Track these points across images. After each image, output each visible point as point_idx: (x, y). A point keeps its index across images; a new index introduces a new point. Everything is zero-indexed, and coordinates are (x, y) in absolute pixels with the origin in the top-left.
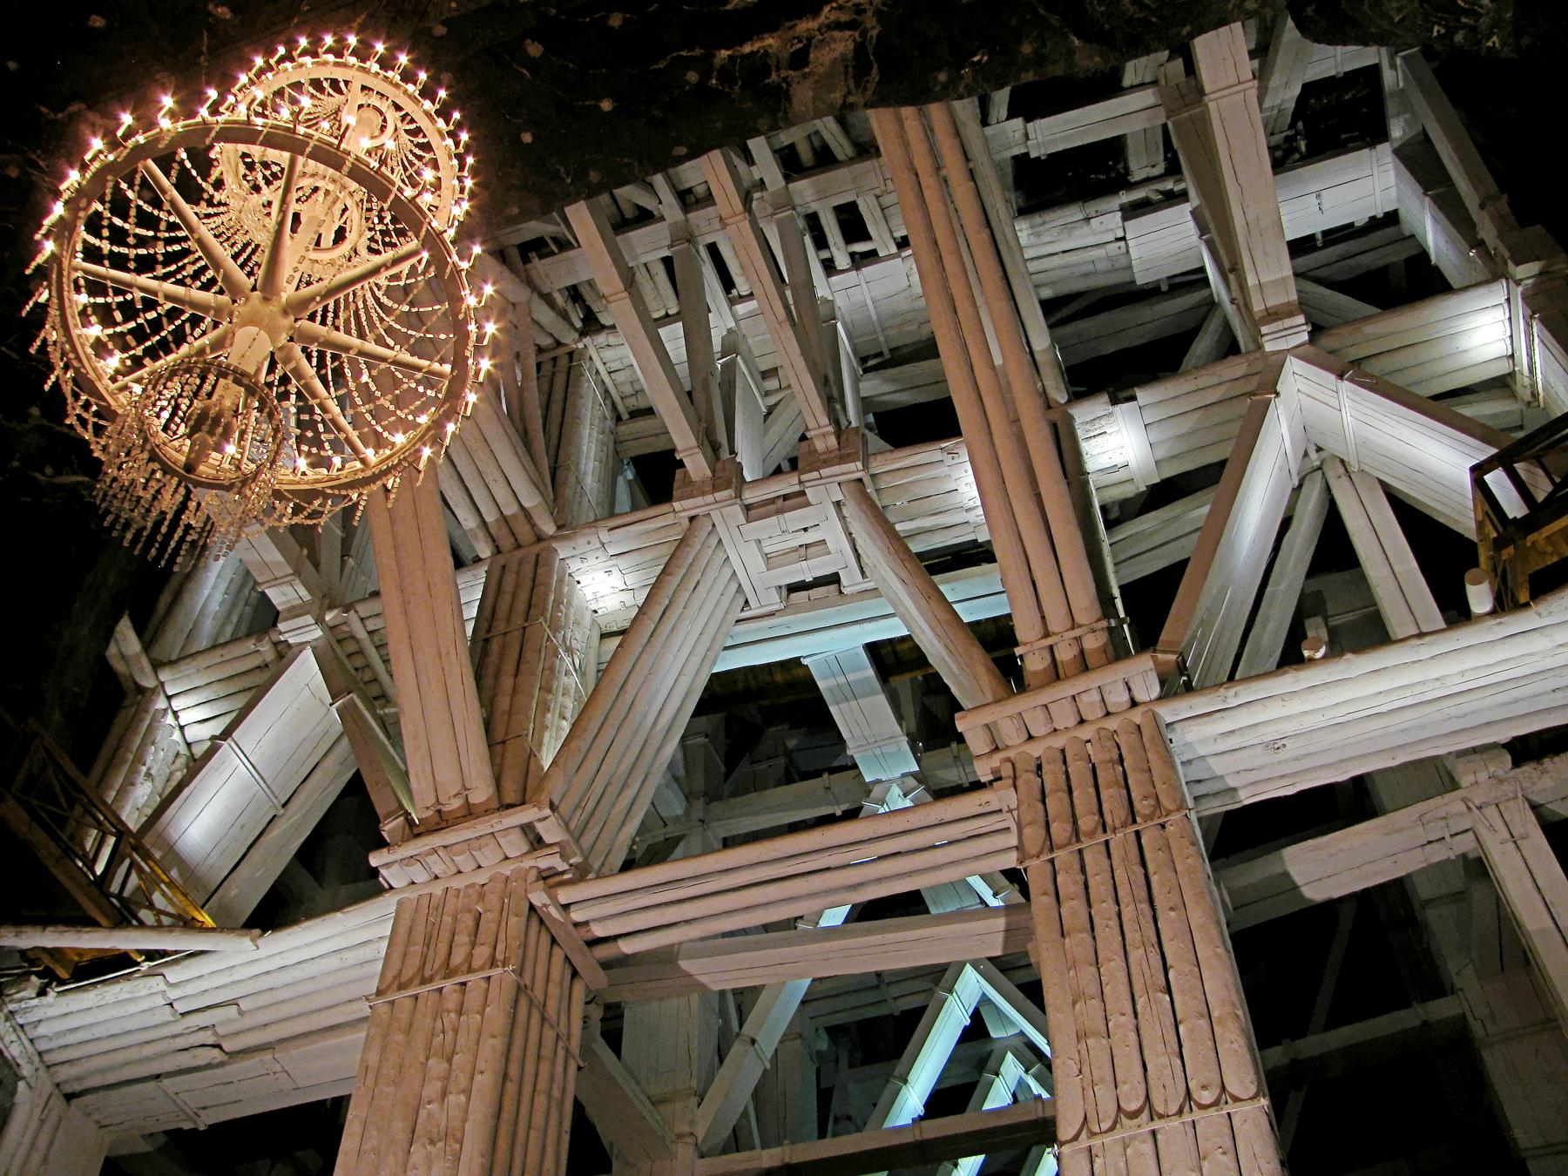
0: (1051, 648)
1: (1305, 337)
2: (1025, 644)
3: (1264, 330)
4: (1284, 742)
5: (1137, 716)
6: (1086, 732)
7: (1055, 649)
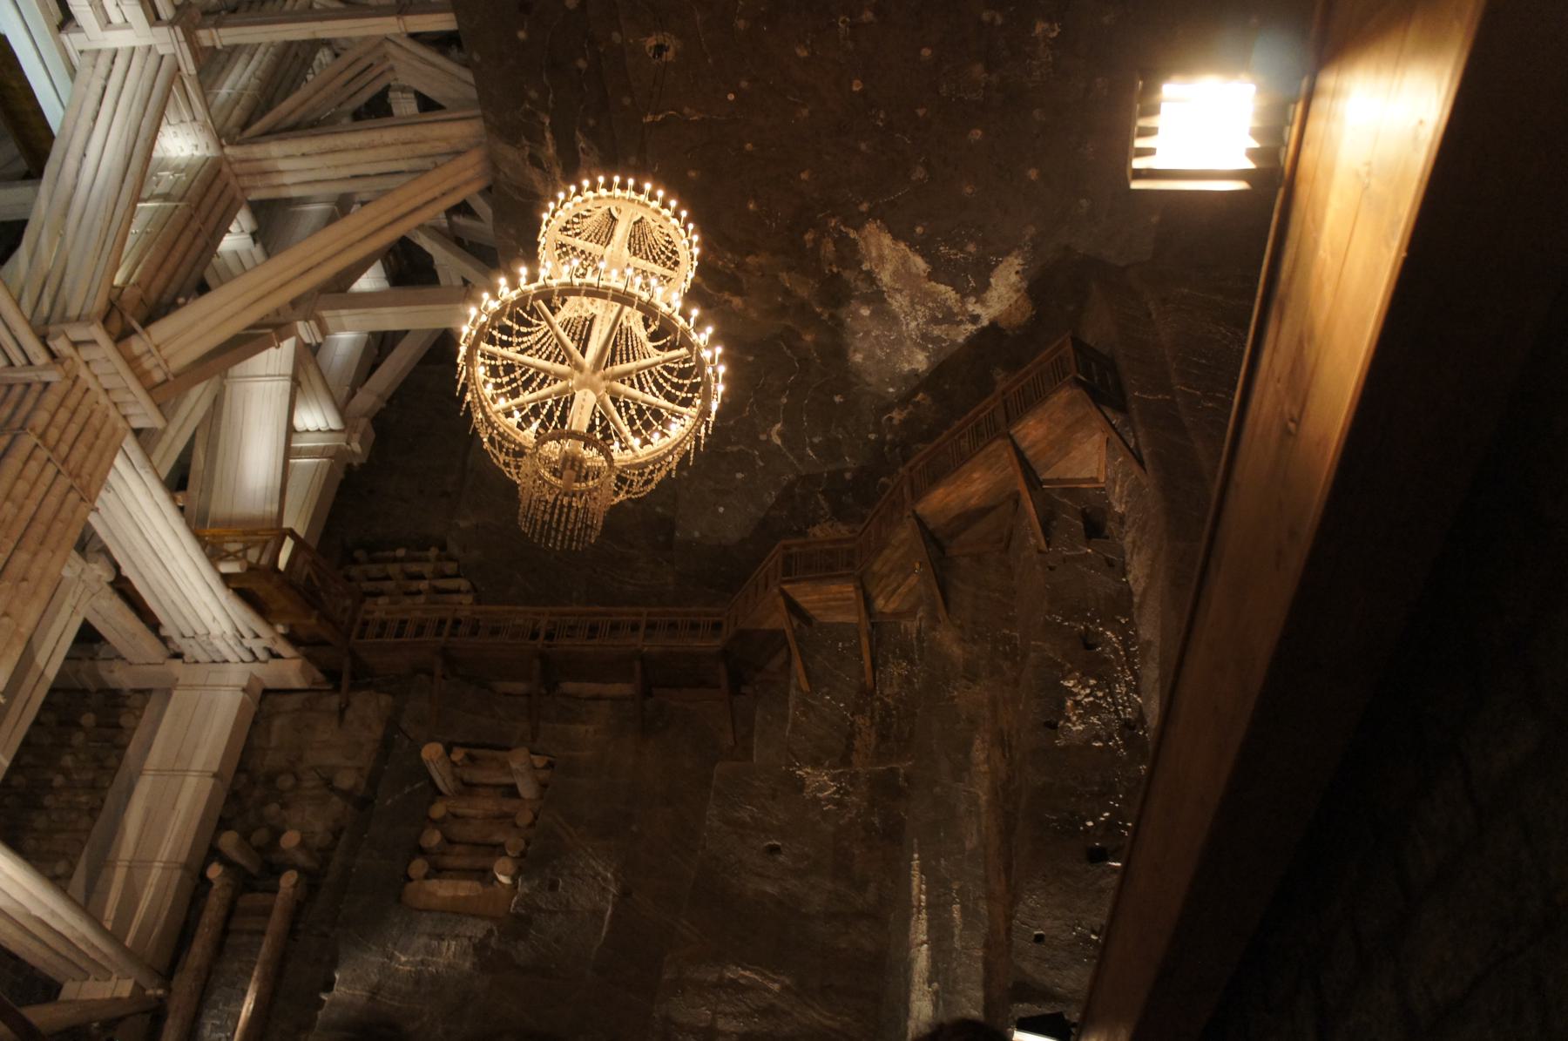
0: (149, 351)
1: (307, 340)
2: (149, 335)
3: (312, 323)
4: (112, 492)
5: (121, 424)
6: (103, 399)
7: (149, 355)
